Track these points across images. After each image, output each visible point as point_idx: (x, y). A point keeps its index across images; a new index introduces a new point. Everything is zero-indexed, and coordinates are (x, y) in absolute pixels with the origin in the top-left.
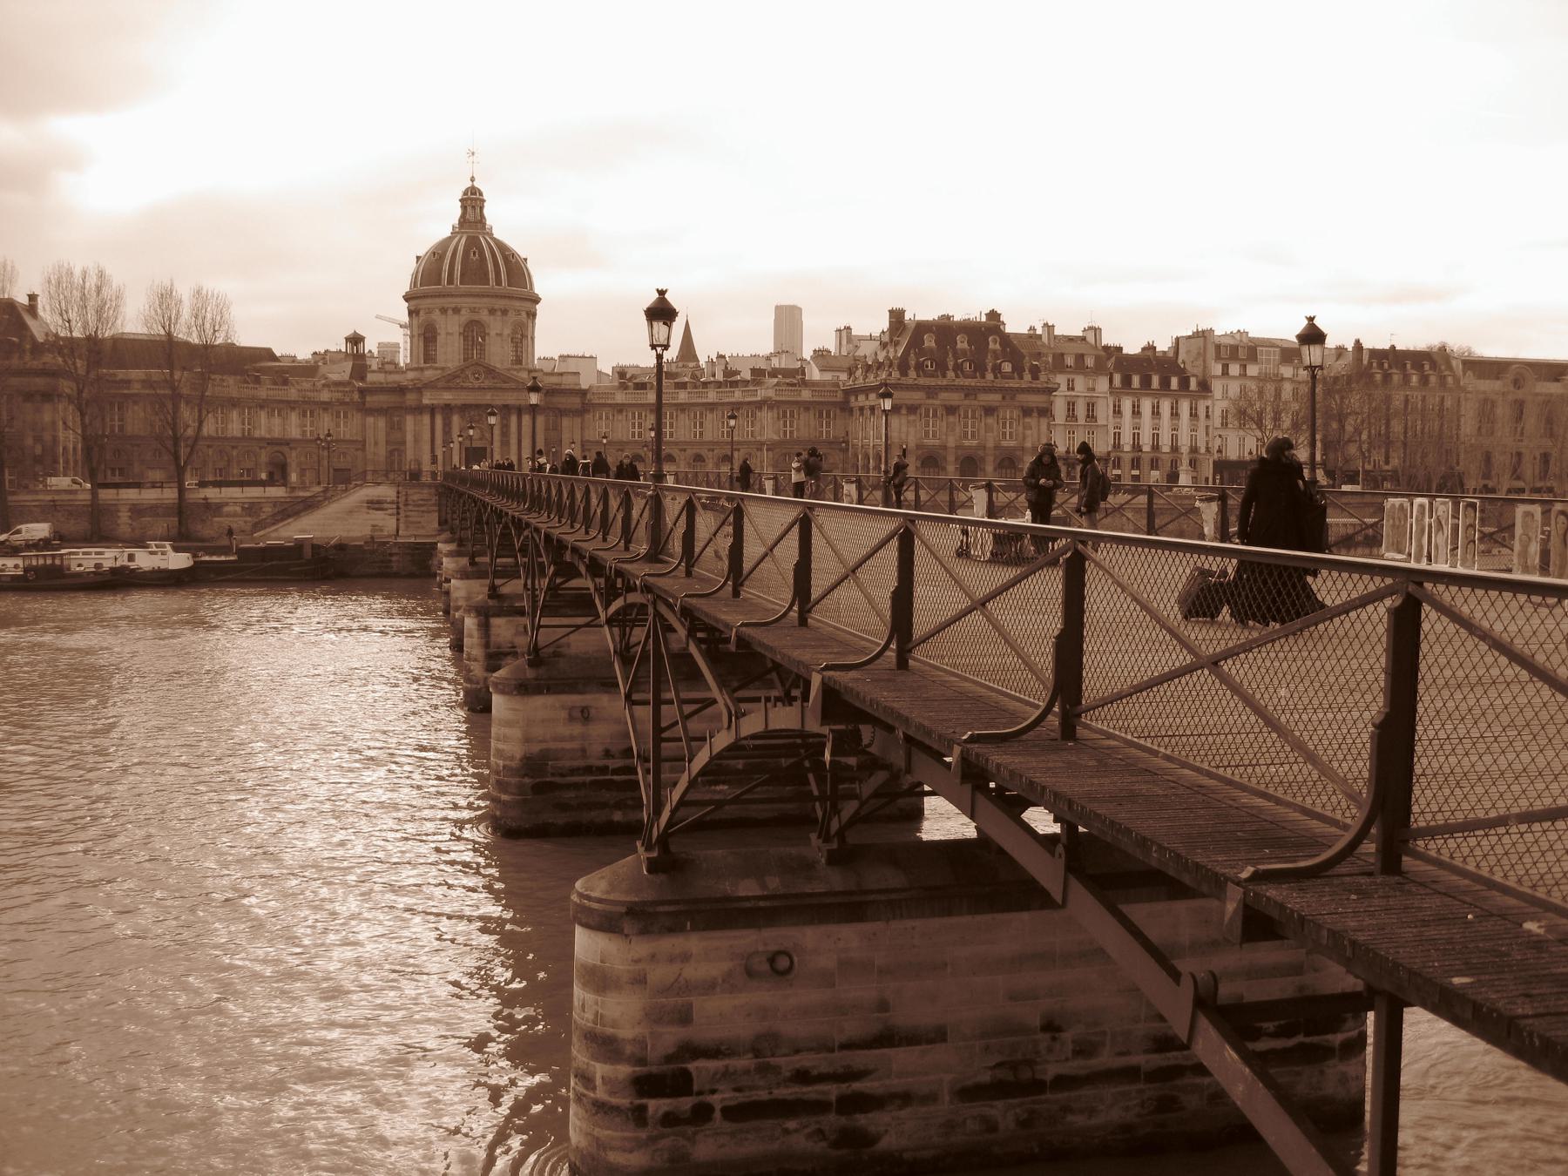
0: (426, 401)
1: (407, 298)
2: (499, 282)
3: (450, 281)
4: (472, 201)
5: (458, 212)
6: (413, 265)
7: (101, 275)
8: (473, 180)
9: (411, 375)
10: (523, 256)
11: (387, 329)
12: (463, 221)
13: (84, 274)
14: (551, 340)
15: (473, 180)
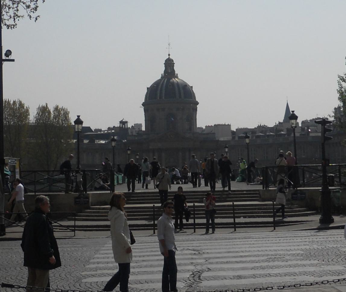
0: (151, 147)
1: (143, 105)
2: (180, 97)
3: (160, 98)
4: (169, 64)
5: (163, 68)
6: (146, 91)
7: (20, 102)
8: (169, 55)
9: (145, 137)
10: (191, 85)
11: (137, 118)
12: (165, 72)
13: (14, 102)
14: (204, 119)
15: (169, 55)
